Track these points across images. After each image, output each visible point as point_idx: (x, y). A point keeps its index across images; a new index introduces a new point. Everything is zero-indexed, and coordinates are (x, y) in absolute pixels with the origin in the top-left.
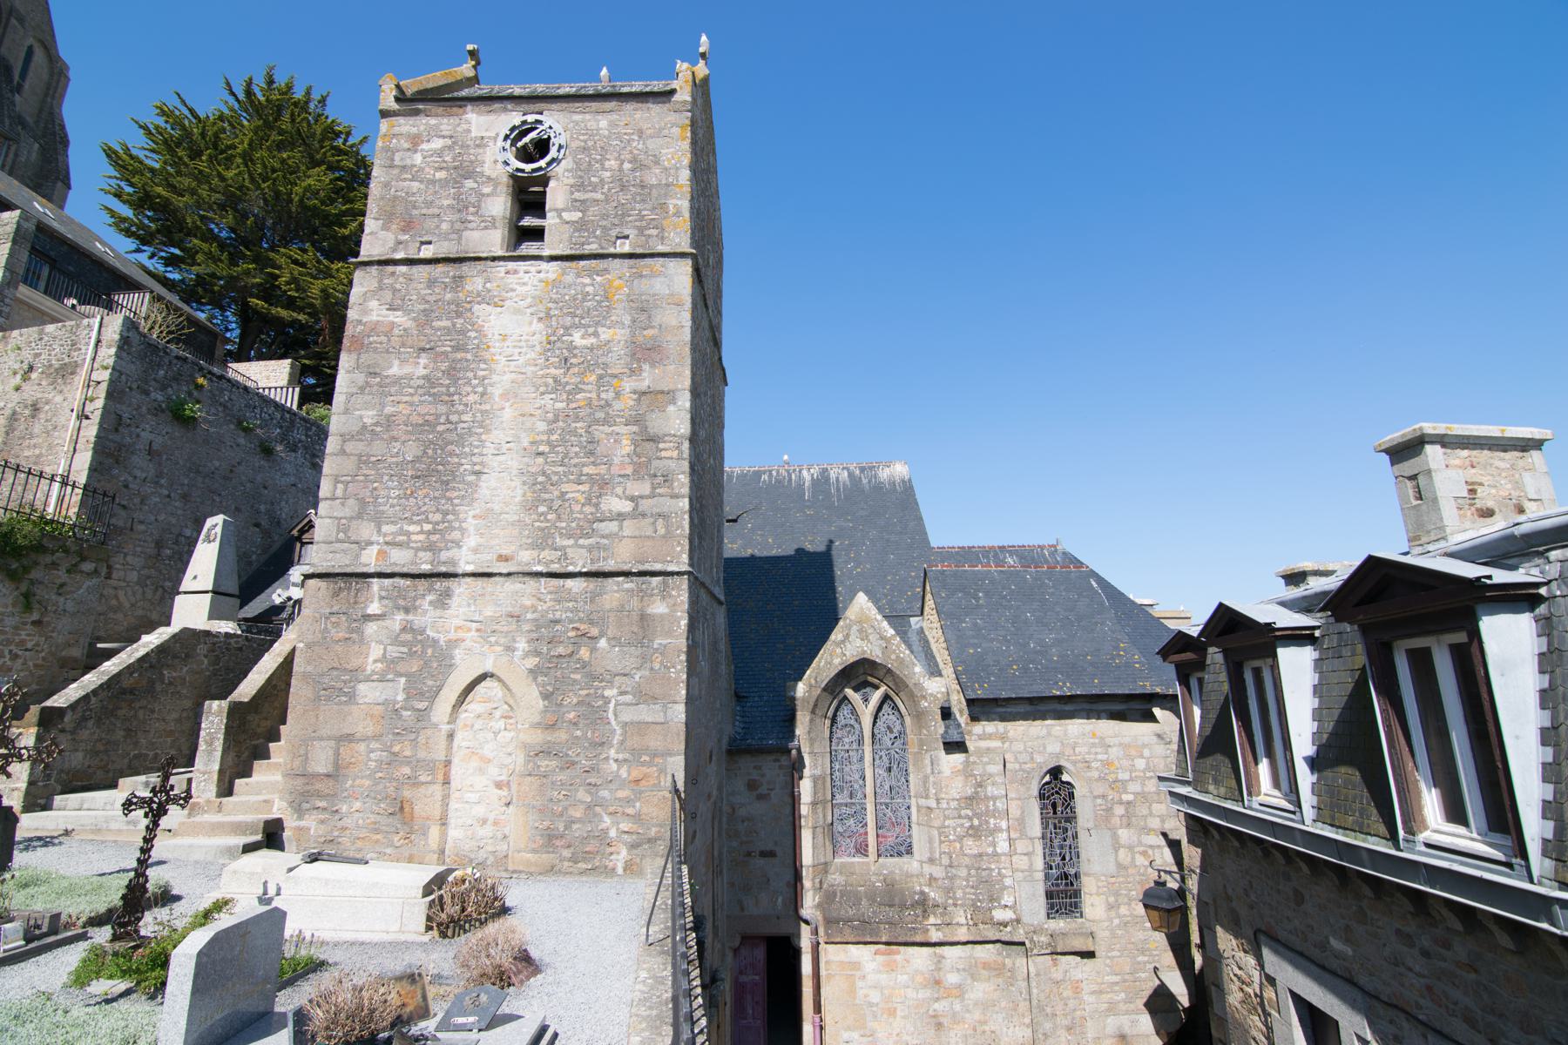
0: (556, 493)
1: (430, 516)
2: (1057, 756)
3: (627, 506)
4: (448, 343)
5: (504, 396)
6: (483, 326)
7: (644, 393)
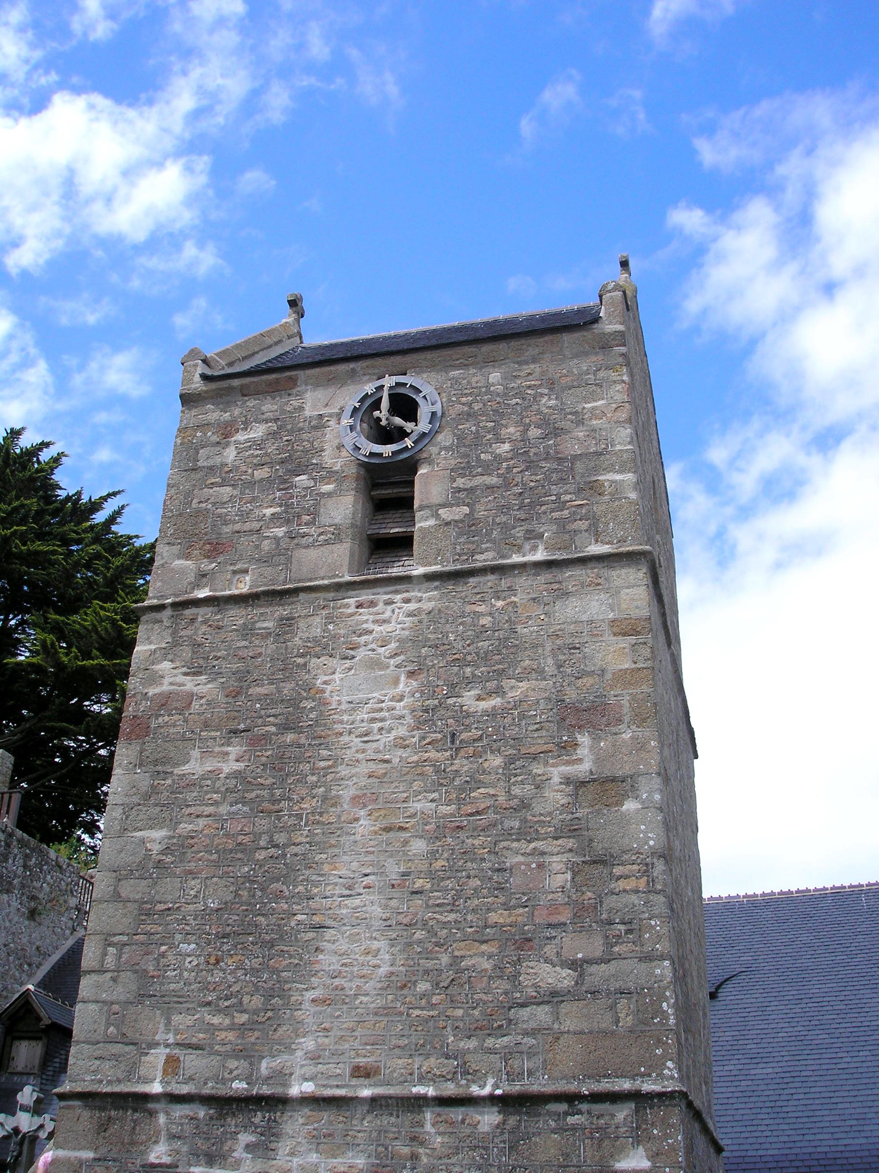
0: (445, 959)
1: (246, 999)
3: (564, 978)
4: (271, 719)
5: (355, 800)
6: (323, 691)
7: (583, 783)
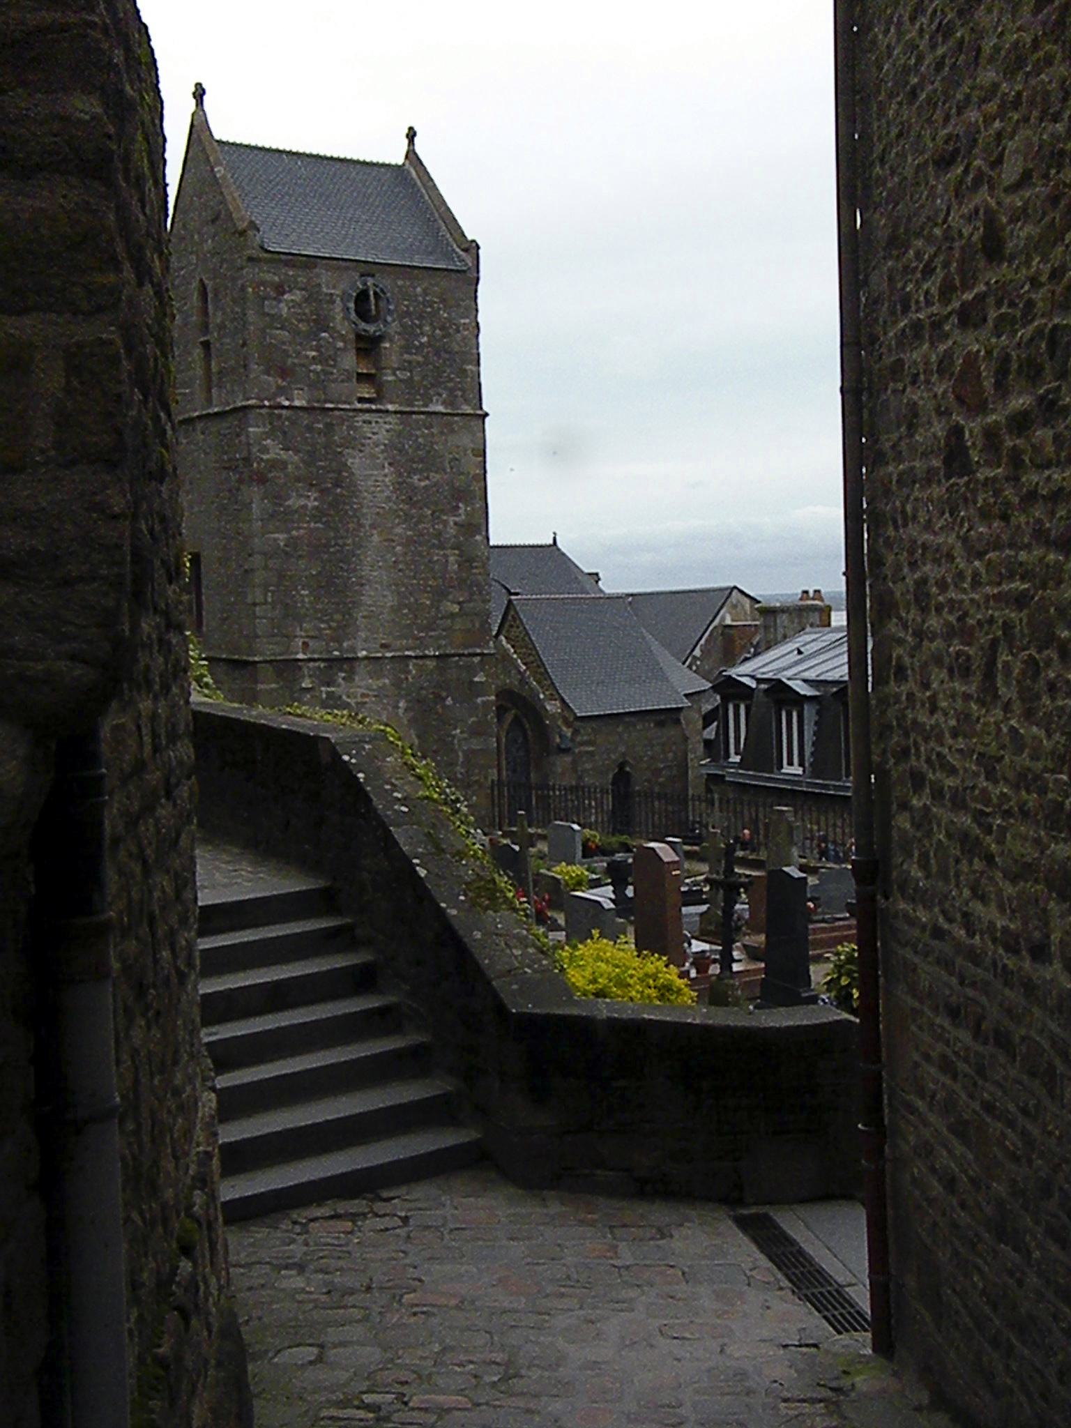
2: (624, 754)
3: (456, 608)
5: (373, 526)
